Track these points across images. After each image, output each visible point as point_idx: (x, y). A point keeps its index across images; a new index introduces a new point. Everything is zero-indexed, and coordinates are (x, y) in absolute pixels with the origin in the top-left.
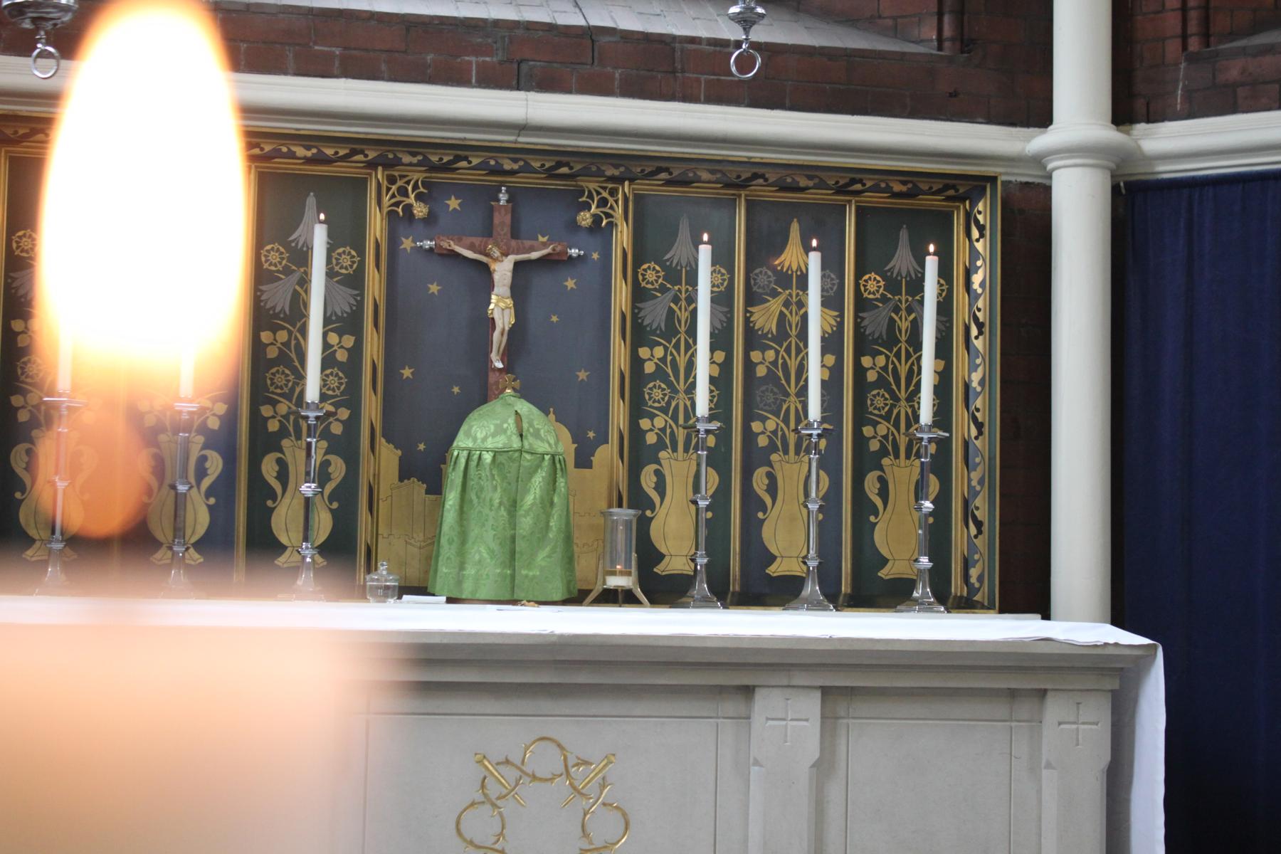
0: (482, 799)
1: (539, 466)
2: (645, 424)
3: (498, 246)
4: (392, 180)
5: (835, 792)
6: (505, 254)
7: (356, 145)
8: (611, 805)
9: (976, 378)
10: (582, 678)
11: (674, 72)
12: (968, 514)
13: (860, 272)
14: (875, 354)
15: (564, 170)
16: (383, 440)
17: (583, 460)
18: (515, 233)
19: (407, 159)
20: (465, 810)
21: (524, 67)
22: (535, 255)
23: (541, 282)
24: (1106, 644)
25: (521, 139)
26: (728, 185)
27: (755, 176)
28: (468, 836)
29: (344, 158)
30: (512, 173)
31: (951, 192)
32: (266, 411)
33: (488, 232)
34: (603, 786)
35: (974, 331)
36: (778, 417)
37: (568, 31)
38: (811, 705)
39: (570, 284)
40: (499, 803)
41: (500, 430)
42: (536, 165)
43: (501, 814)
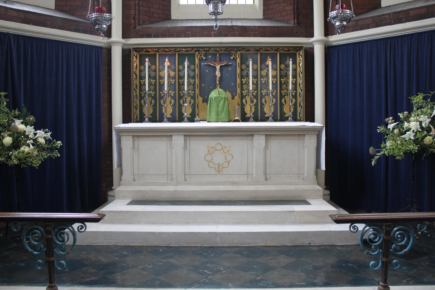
0: (209, 153)
1: (222, 99)
2: (243, 92)
3: (217, 63)
4: (199, 53)
5: (268, 152)
6: (218, 65)
7: (193, 48)
8: (230, 154)
9: (301, 81)
10: (224, 134)
11: (247, 32)
12: (300, 105)
13: (280, 64)
14: (283, 78)
15: (228, 50)
16: (199, 96)
17: (233, 98)
18: (220, 61)
19: (201, 50)
20: (206, 155)
21: (221, 33)
22: (223, 64)
23: (225, 69)
24: (315, 126)
25: (221, 45)
26: (256, 51)
27: (261, 49)
28: (206, 160)
29: (191, 50)
30: (219, 51)
31: (296, 50)
32: (181, 92)
33: (216, 61)
34: (229, 151)
35: (300, 74)
36: (266, 90)
37: (229, 26)
38: (263, 137)
39: (230, 69)
40: (211, 154)
41: (216, 94)
42: (223, 49)
43: (212, 156)
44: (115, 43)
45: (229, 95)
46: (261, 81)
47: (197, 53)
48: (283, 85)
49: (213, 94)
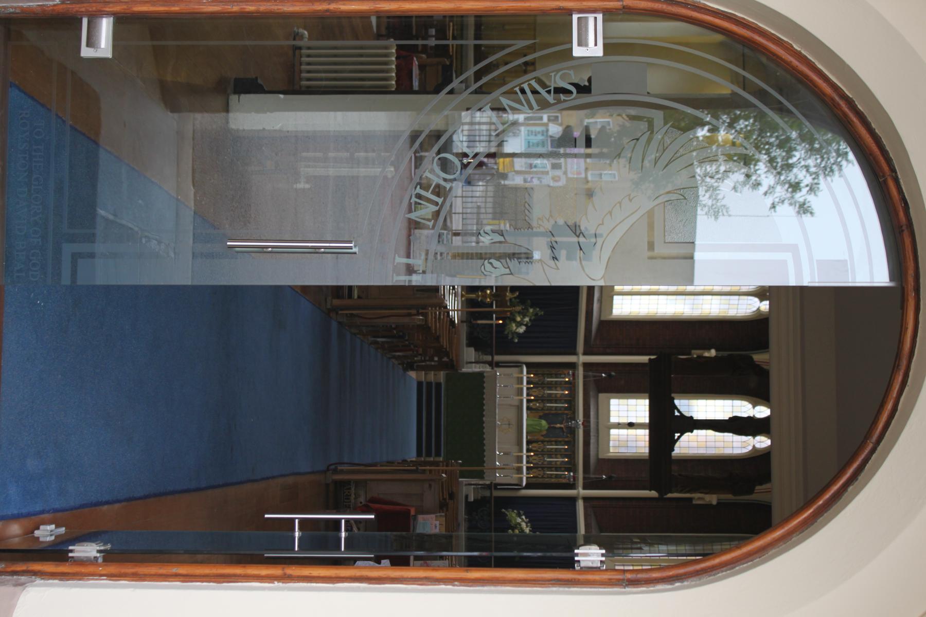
7: (575, 409)
13: (565, 467)
17: (542, 436)
44: (578, 359)
45: (545, 433)
46: (553, 454)
47: (572, 412)
48: (550, 469)
49: (544, 423)
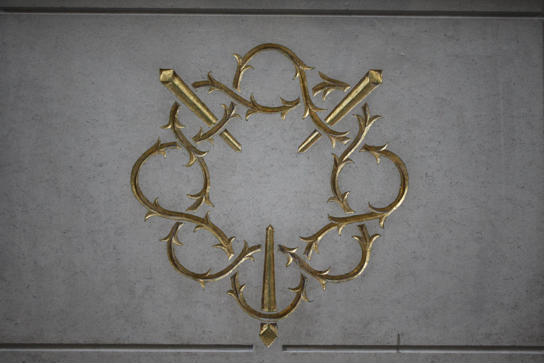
0: (173, 139)
8: (377, 149)
20: (146, 155)
34: (363, 120)
40: (199, 145)
43: (202, 163)
